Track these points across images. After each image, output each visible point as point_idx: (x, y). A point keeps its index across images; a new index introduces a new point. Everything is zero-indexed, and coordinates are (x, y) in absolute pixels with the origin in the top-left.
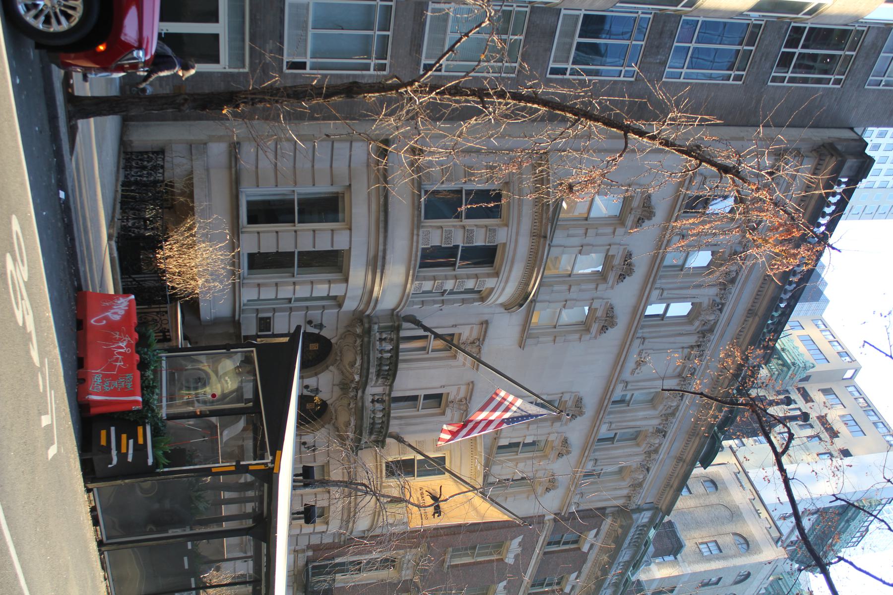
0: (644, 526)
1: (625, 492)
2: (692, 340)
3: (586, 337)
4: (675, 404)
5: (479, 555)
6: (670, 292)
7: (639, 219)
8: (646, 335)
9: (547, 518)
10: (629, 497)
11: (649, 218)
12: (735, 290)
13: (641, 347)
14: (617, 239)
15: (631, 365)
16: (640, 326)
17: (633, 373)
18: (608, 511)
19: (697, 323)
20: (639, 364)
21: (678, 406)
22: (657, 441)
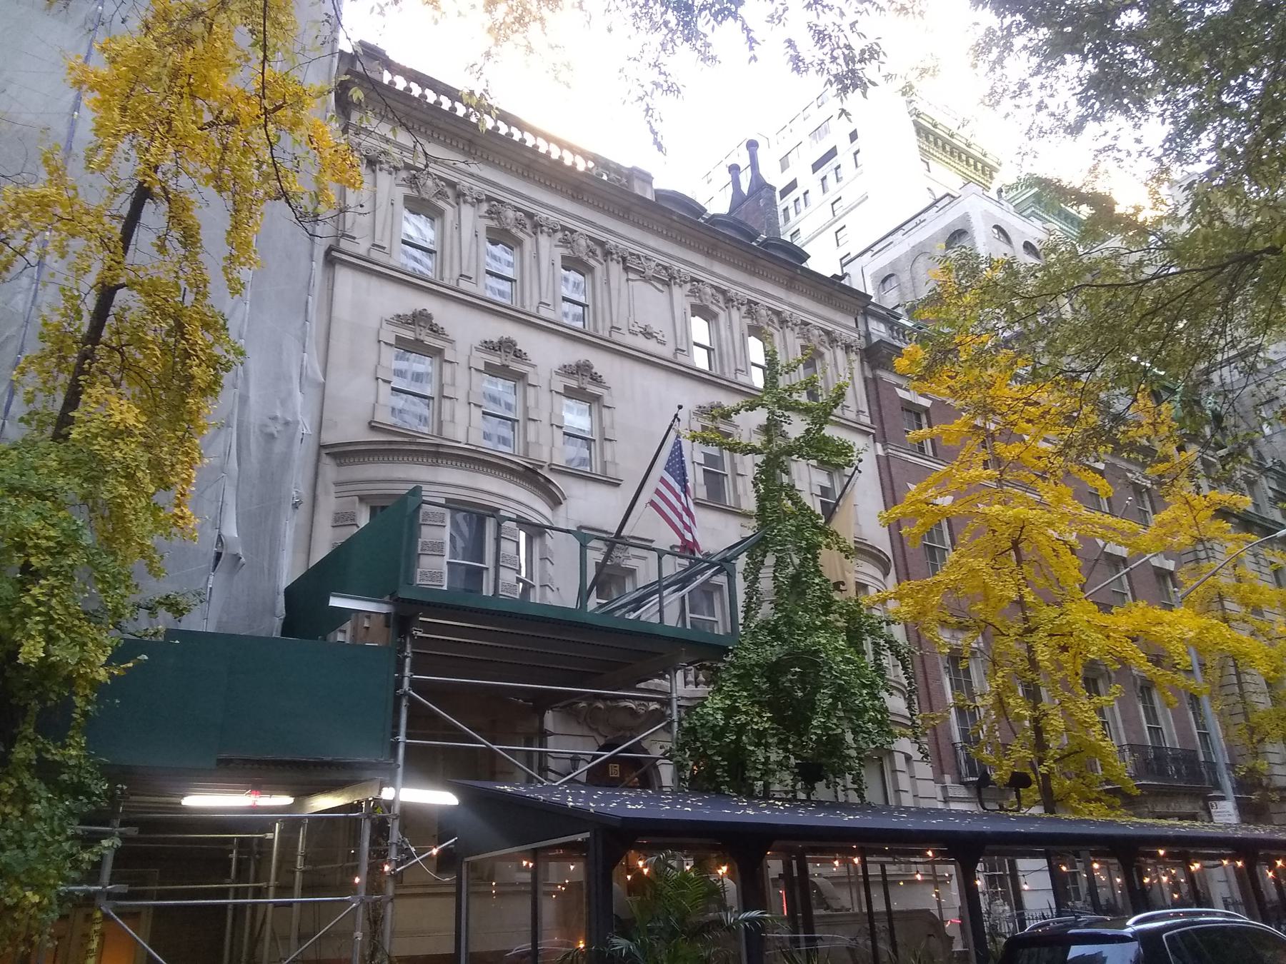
0: (891, 329)
1: (840, 353)
2: (616, 269)
4: (708, 290)
5: (943, 543)
6: (543, 294)
8: (608, 325)
9: (881, 452)
10: (848, 348)
11: (429, 317)
12: (543, 214)
14: (462, 360)
15: (650, 346)
17: (663, 343)
19: (592, 262)
20: (647, 334)
22: (763, 312)
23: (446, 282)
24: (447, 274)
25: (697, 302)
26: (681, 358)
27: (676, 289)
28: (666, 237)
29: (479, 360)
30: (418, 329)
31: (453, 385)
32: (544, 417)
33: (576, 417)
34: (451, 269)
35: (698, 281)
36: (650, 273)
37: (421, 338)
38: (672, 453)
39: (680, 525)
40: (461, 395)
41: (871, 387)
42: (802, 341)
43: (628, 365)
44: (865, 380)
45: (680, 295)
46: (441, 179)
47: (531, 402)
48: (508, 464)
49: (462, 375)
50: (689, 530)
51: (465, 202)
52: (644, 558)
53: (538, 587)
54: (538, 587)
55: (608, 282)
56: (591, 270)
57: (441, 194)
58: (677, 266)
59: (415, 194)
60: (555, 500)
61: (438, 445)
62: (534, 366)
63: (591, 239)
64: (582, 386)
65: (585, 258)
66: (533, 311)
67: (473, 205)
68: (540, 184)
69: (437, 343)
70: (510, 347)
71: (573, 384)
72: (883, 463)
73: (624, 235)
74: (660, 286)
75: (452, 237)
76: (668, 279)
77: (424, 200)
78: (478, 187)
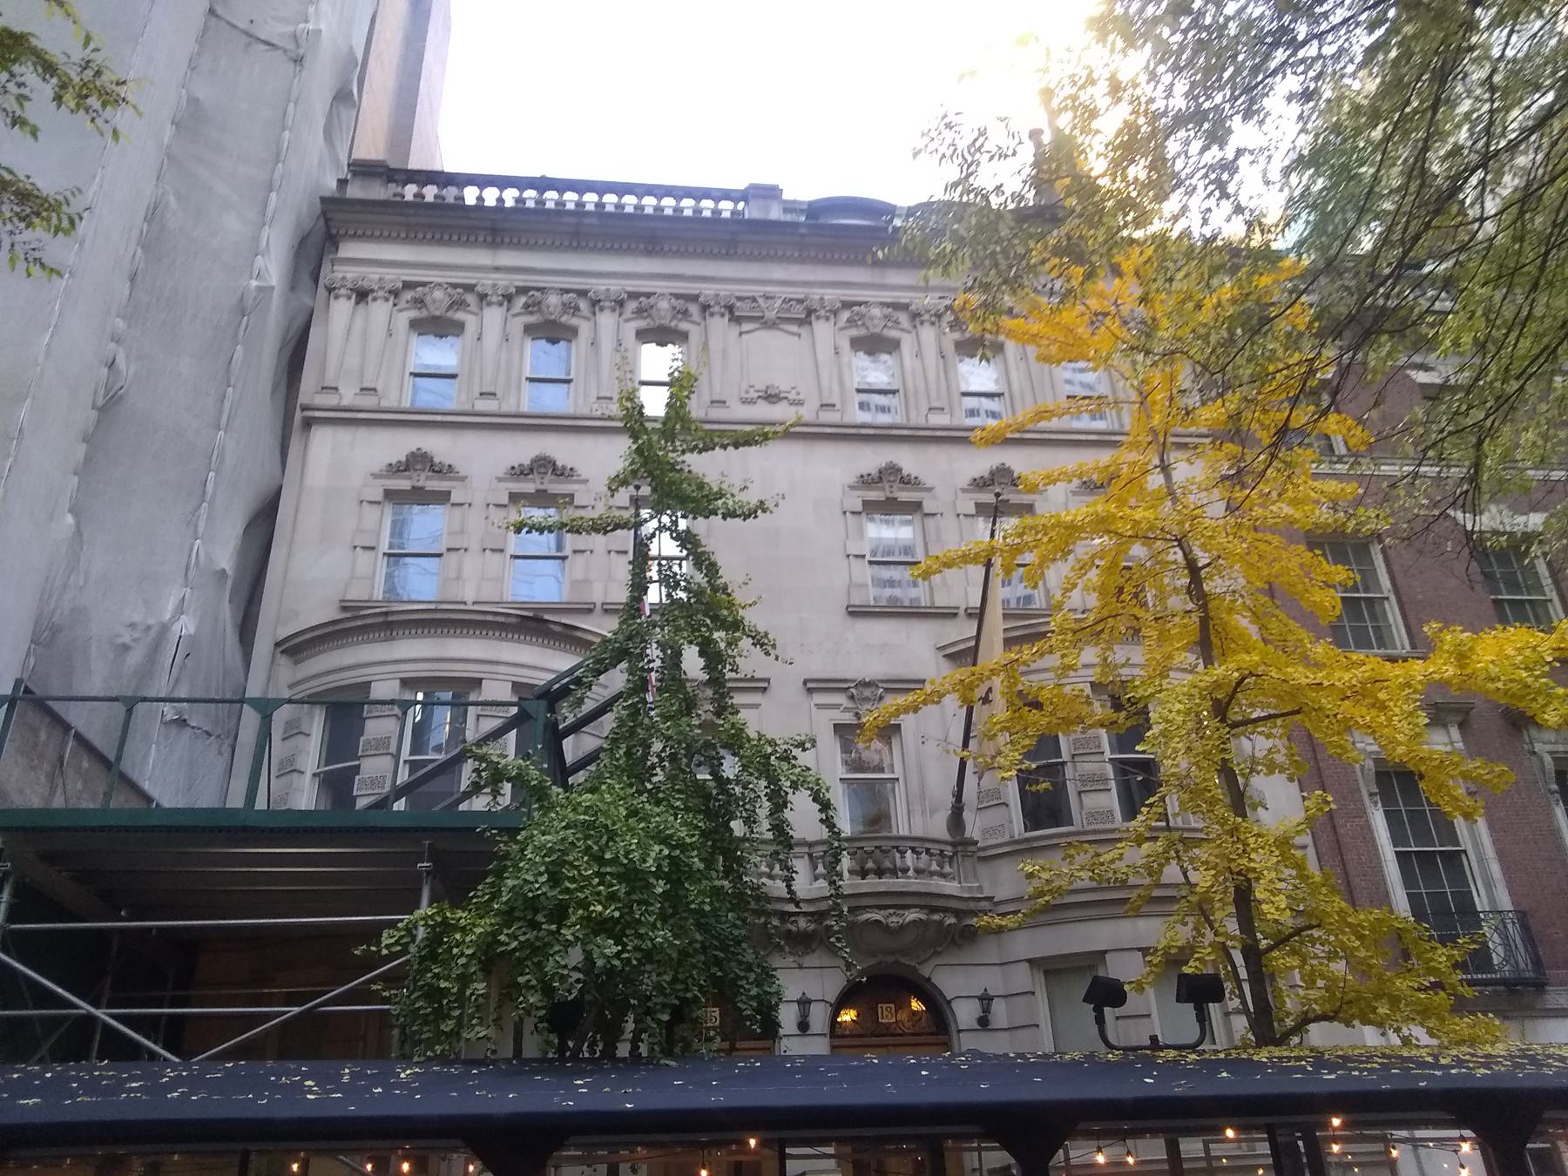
4: (876, 312)
12: (599, 286)
17: (800, 403)
19: (684, 326)
20: (772, 397)
21: (883, 304)
24: (913, 414)
25: (863, 332)
28: (802, 260)
30: (415, 475)
35: (860, 304)
36: (771, 315)
37: (420, 484)
45: (823, 330)
46: (455, 286)
52: (756, 706)
57: (460, 304)
58: (816, 293)
59: (424, 313)
61: (386, 614)
63: (677, 296)
65: (564, 319)
68: (595, 250)
74: (794, 328)
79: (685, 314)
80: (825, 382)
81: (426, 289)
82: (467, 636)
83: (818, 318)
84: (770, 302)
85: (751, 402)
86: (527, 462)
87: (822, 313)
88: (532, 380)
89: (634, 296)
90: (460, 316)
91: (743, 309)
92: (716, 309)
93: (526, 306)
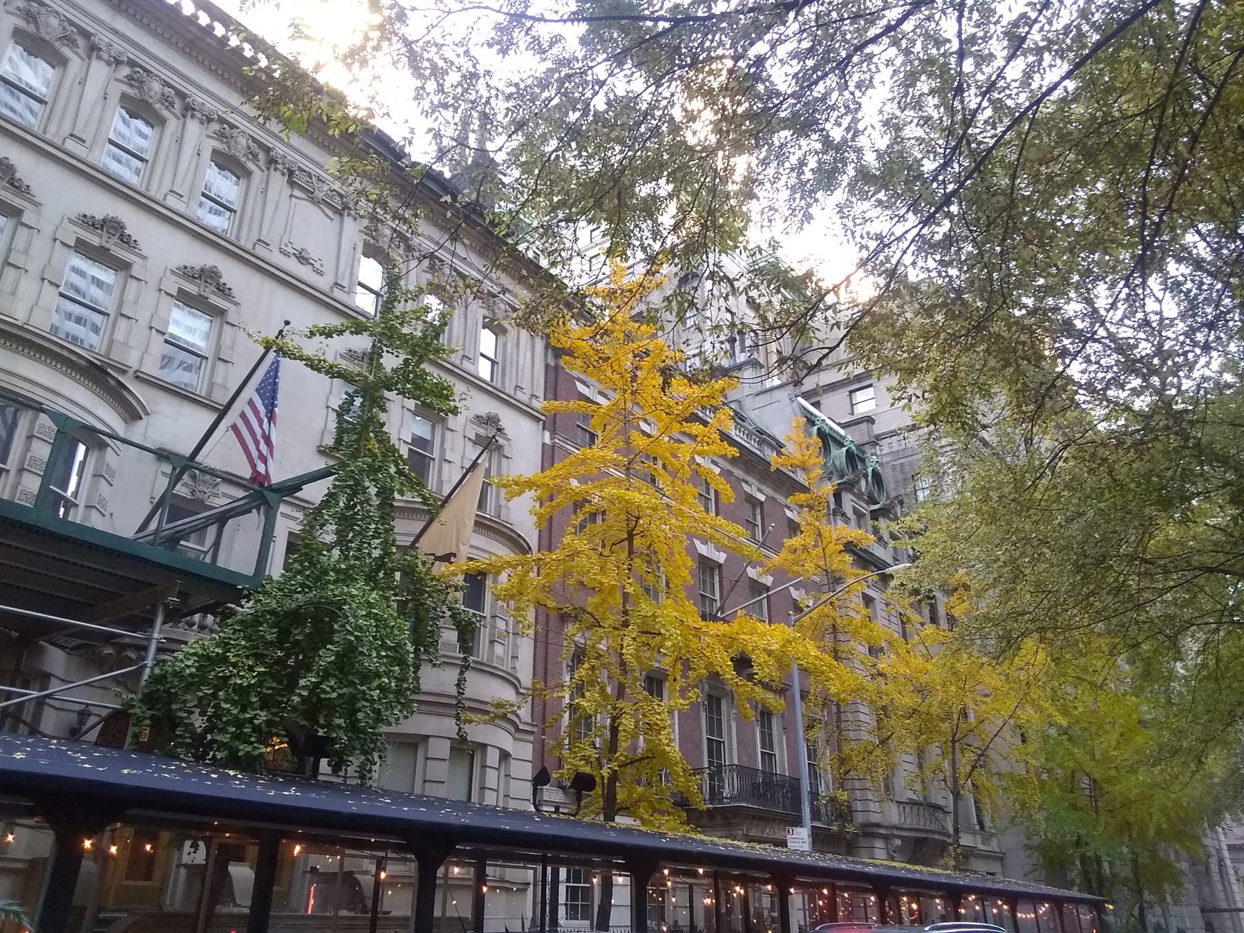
2: (278, 181)
3: (232, 316)
6: (178, 183)
7: (12, 184)
8: (254, 236)
9: (547, 441)
12: (198, 98)
13: (276, 251)
14: (47, 230)
15: (304, 272)
16: (236, 242)
17: (320, 273)
18: (552, 362)
20: (302, 258)
23: (48, 137)
26: (338, 294)
27: (348, 221)
29: (71, 233)
31: (26, 253)
32: (144, 317)
33: (189, 327)
34: (60, 125)
36: (320, 195)
38: (268, 372)
39: (255, 454)
40: (34, 267)
41: (552, 375)
42: (486, 312)
43: (270, 286)
44: (547, 366)
46: (72, 23)
47: (130, 296)
48: (65, 353)
49: (40, 246)
50: (264, 460)
51: (99, 58)
53: (81, 507)
54: (81, 507)
55: (265, 192)
56: (248, 174)
57: (68, 40)
59: (31, 29)
60: (132, 414)
62: (144, 258)
64: (203, 293)
66: (159, 197)
67: (108, 63)
68: (201, 64)
69: (18, 202)
70: (116, 229)
71: (192, 289)
72: (548, 451)
73: (297, 148)
74: (330, 213)
75: (71, 91)
76: (341, 209)
77: (44, 40)
78: (119, 46)
79: (255, 157)
80: (342, 267)
81: (43, 10)
82: (38, 361)
83: (349, 215)
84: (321, 184)
85: (287, 254)
86: (99, 217)
87: (353, 213)
88: (111, 142)
89: (222, 121)
90: (66, 51)
91: (300, 179)
92: (280, 167)
93: (130, 78)
